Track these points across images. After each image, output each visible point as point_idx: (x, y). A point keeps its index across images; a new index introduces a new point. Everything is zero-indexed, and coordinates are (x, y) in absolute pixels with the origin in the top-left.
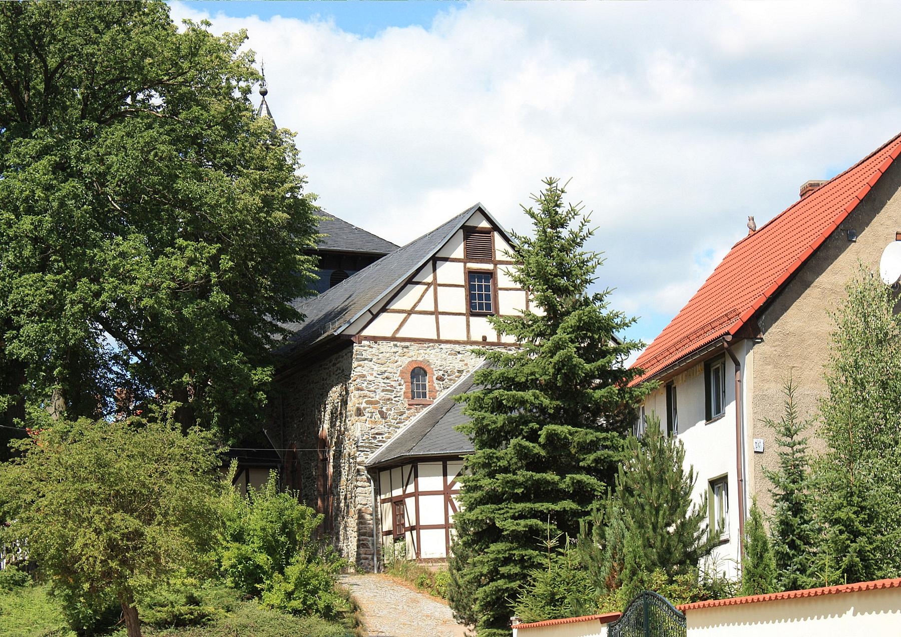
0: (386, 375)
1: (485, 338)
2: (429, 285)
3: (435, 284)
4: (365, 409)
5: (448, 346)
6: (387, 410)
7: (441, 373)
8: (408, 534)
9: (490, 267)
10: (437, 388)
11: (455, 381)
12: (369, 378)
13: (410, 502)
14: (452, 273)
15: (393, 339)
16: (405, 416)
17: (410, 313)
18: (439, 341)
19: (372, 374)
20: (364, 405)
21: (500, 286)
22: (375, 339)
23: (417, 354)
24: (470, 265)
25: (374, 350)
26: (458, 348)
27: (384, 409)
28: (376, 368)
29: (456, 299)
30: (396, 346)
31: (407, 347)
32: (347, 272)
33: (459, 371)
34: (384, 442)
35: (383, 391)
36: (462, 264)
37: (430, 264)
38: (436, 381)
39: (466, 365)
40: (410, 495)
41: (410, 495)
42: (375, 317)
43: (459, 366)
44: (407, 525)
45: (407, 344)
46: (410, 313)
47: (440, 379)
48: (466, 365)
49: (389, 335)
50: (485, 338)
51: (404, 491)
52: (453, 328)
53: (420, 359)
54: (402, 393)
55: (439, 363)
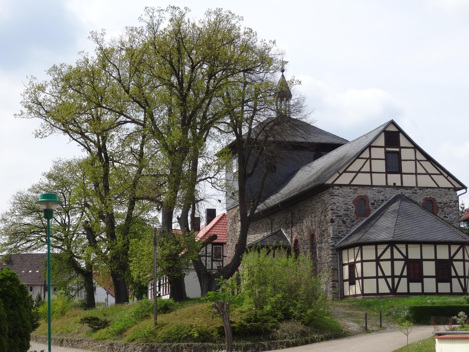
0: (346, 202)
1: (395, 184)
2: (367, 159)
3: (370, 159)
4: (335, 219)
5: (377, 188)
6: (346, 219)
7: (373, 201)
8: (357, 281)
9: (398, 150)
10: (371, 209)
11: (380, 205)
12: (338, 204)
13: (358, 266)
14: (379, 153)
15: (350, 185)
16: (355, 222)
17: (359, 172)
18: (372, 186)
19: (339, 203)
20: (335, 217)
21: (403, 158)
22: (341, 186)
23: (361, 192)
24: (387, 149)
25: (340, 191)
26: (382, 189)
27: (344, 219)
28: (341, 199)
29: (380, 166)
30: (351, 188)
31: (356, 189)
32: (322, 153)
33: (382, 200)
34: (345, 235)
35: (344, 210)
36: (384, 149)
37: (368, 150)
38: (370, 206)
39: (385, 197)
40: (358, 262)
41: (358, 262)
42: (341, 175)
43: (382, 198)
44: (356, 277)
45: (356, 188)
46: (359, 172)
47: (373, 204)
48: (385, 197)
49: (347, 183)
50: (395, 184)
51: (355, 260)
52: (379, 180)
53: (363, 195)
54: (354, 211)
55: (372, 196)
